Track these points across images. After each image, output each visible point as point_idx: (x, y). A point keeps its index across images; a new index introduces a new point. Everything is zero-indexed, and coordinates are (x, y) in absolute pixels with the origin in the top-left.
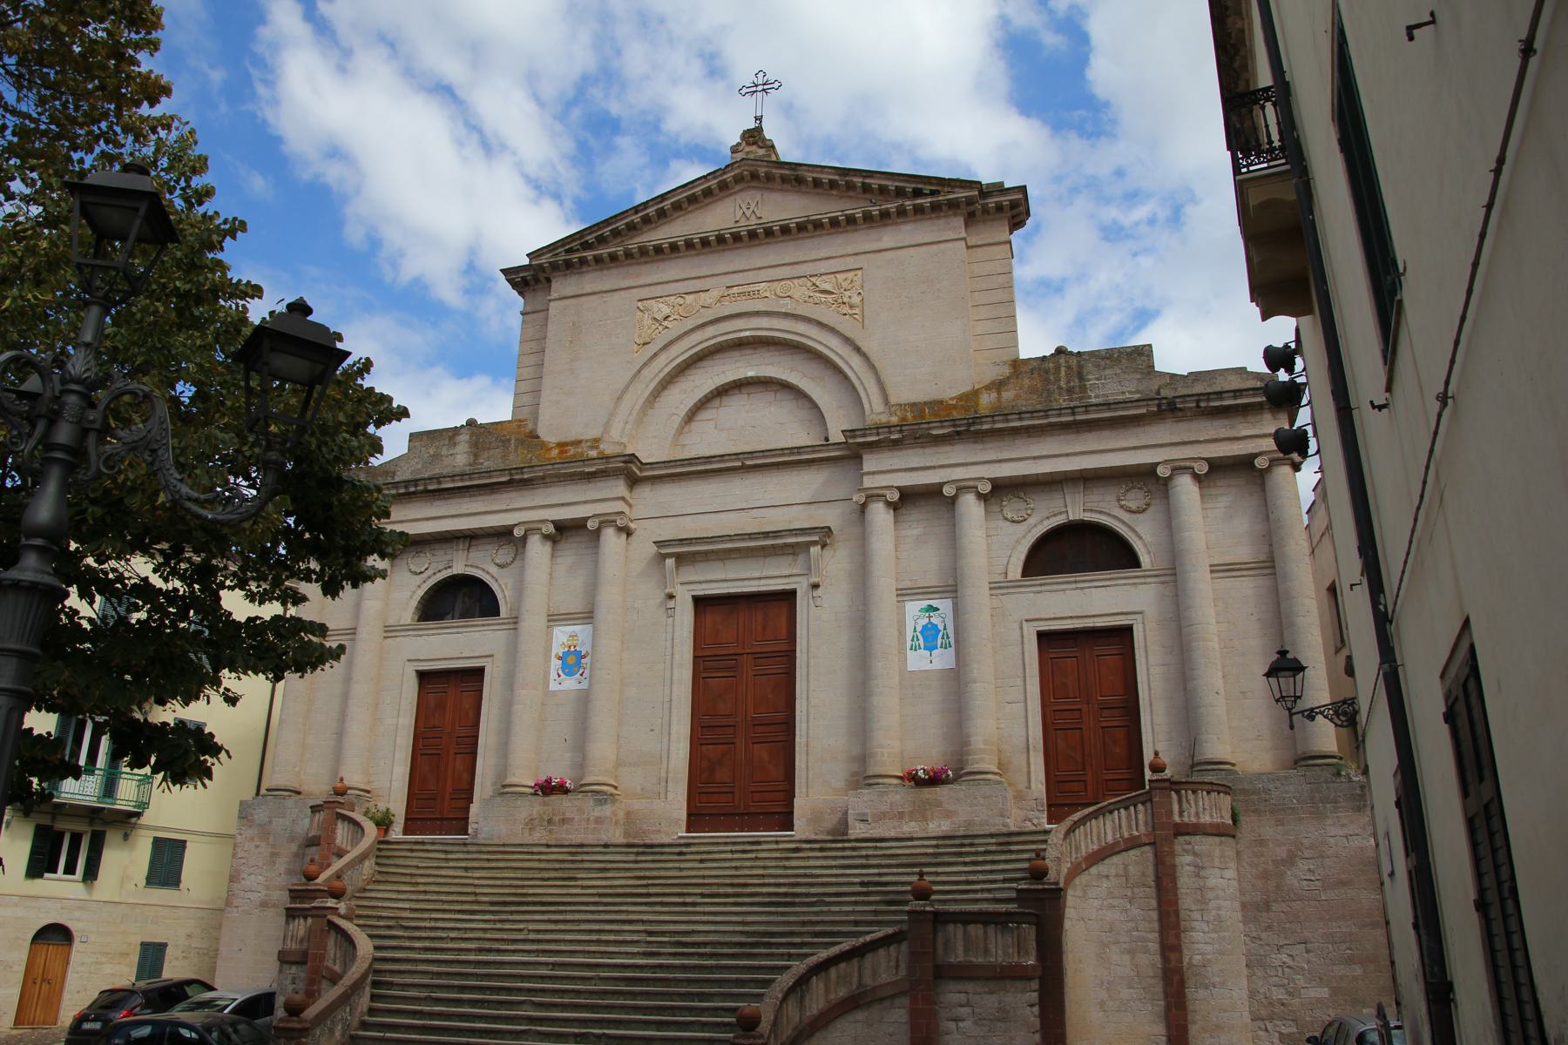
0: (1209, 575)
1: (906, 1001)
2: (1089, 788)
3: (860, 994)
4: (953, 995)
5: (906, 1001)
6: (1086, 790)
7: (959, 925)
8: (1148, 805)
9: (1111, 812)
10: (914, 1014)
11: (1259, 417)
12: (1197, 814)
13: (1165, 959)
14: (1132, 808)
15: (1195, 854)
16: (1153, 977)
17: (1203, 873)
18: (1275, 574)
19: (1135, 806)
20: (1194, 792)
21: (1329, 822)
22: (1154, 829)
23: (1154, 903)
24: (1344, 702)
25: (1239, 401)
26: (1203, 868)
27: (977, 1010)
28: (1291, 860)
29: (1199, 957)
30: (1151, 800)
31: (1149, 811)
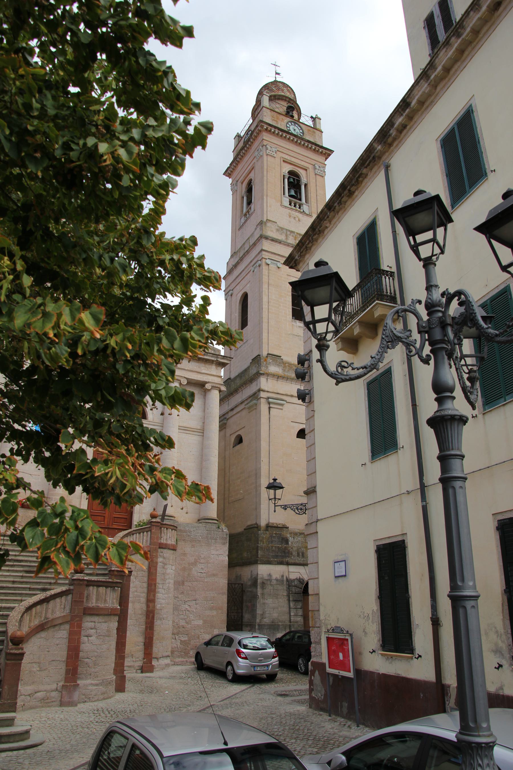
0: (177, 430)
1: (67, 626)
2: (106, 520)
3: (45, 623)
4: (88, 623)
5: (67, 626)
6: (104, 521)
7: (95, 587)
8: (149, 533)
9: (133, 534)
10: (71, 633)
11: (210, 366)
12: (166, 539)
13: (148, 606)
14: (142, 533)
15: (164, 558)
16: (140, 614)
17: (166, 567)
18: (203, 436)
19: (143, 533)
20: (167, 529)
21: (212, 548)
22: (150, 544)
23: (146, 579)
24: (302, 505)
25: (205, 357)
26: (166, 564)
27: (98, 631)
28: (195, 564)
29: (159, 605)
30: (151, 531)
31: (149, 536)
